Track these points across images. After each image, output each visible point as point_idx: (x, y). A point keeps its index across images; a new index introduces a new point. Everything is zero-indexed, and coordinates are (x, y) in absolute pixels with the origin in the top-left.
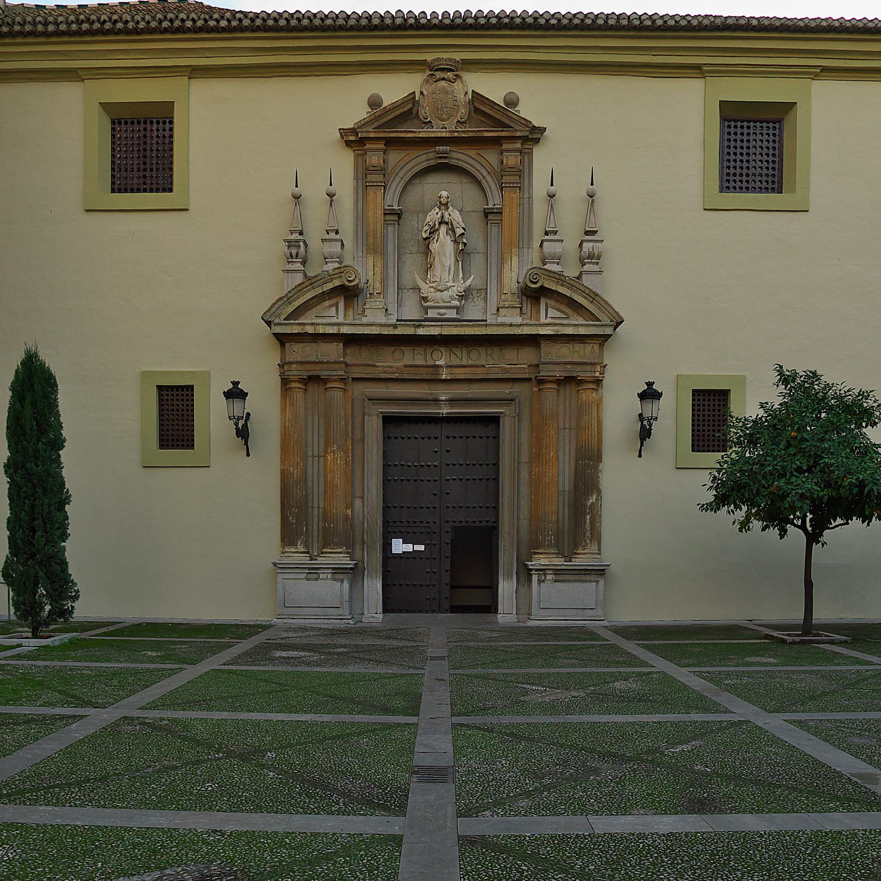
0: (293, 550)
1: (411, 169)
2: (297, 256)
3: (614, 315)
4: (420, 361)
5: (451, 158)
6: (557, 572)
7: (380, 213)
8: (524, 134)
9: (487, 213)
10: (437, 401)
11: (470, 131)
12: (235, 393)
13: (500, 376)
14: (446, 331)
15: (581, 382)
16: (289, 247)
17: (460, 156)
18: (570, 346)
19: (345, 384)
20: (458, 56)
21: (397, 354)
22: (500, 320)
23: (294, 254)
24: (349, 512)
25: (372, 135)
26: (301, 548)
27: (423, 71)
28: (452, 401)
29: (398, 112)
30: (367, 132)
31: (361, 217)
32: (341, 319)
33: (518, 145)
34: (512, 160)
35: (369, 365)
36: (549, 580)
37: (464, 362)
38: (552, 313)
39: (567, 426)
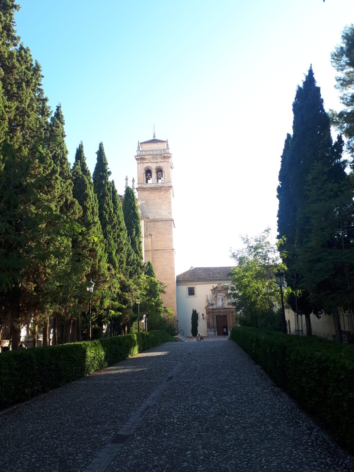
11: (222, 289)
12: (203, 315)
17: (221, 291)
31: (212, 297)
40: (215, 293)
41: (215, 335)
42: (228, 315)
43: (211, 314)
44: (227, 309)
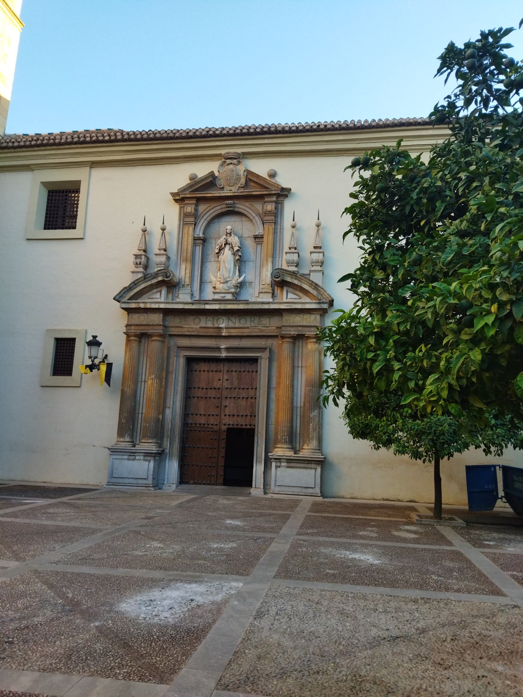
0: (122, 440)
1: (211, 214)
2: (140, 264)
3: (328, 296)
4: (210, 325)
5: (234, 207)
6: (289, 461)
7: (191, 239)
8: (277, 192)
9: (256, 237)
10: (218, 349)
13: (259, 334)
14: (223, 307)
15: (308, 338)
16: (136, 258)
17: (241, 206)
18: (301, 316)
19: (164, 338)
20: (240, 150)
21: (197, 321)
22: (259, 300)
23: (138, 263)
24: (161, 416)
25: (188, 196)
26: (127, 439)
27: (221, 159)
28: (228, 349)
29: (203, 183)
30: (185, 194)
31: (180, 241)
32: (162, 300)
33: (274, 199)
34: (270, 207)
35: (178, 327)
36: (283, 466)
37: (237, 325)
38: (290, 295)
39: (300, 365)
40: (196, 216)
41: (158, 483)
42: (264, 356)
43: (154, 345)
44: (265, 321)
